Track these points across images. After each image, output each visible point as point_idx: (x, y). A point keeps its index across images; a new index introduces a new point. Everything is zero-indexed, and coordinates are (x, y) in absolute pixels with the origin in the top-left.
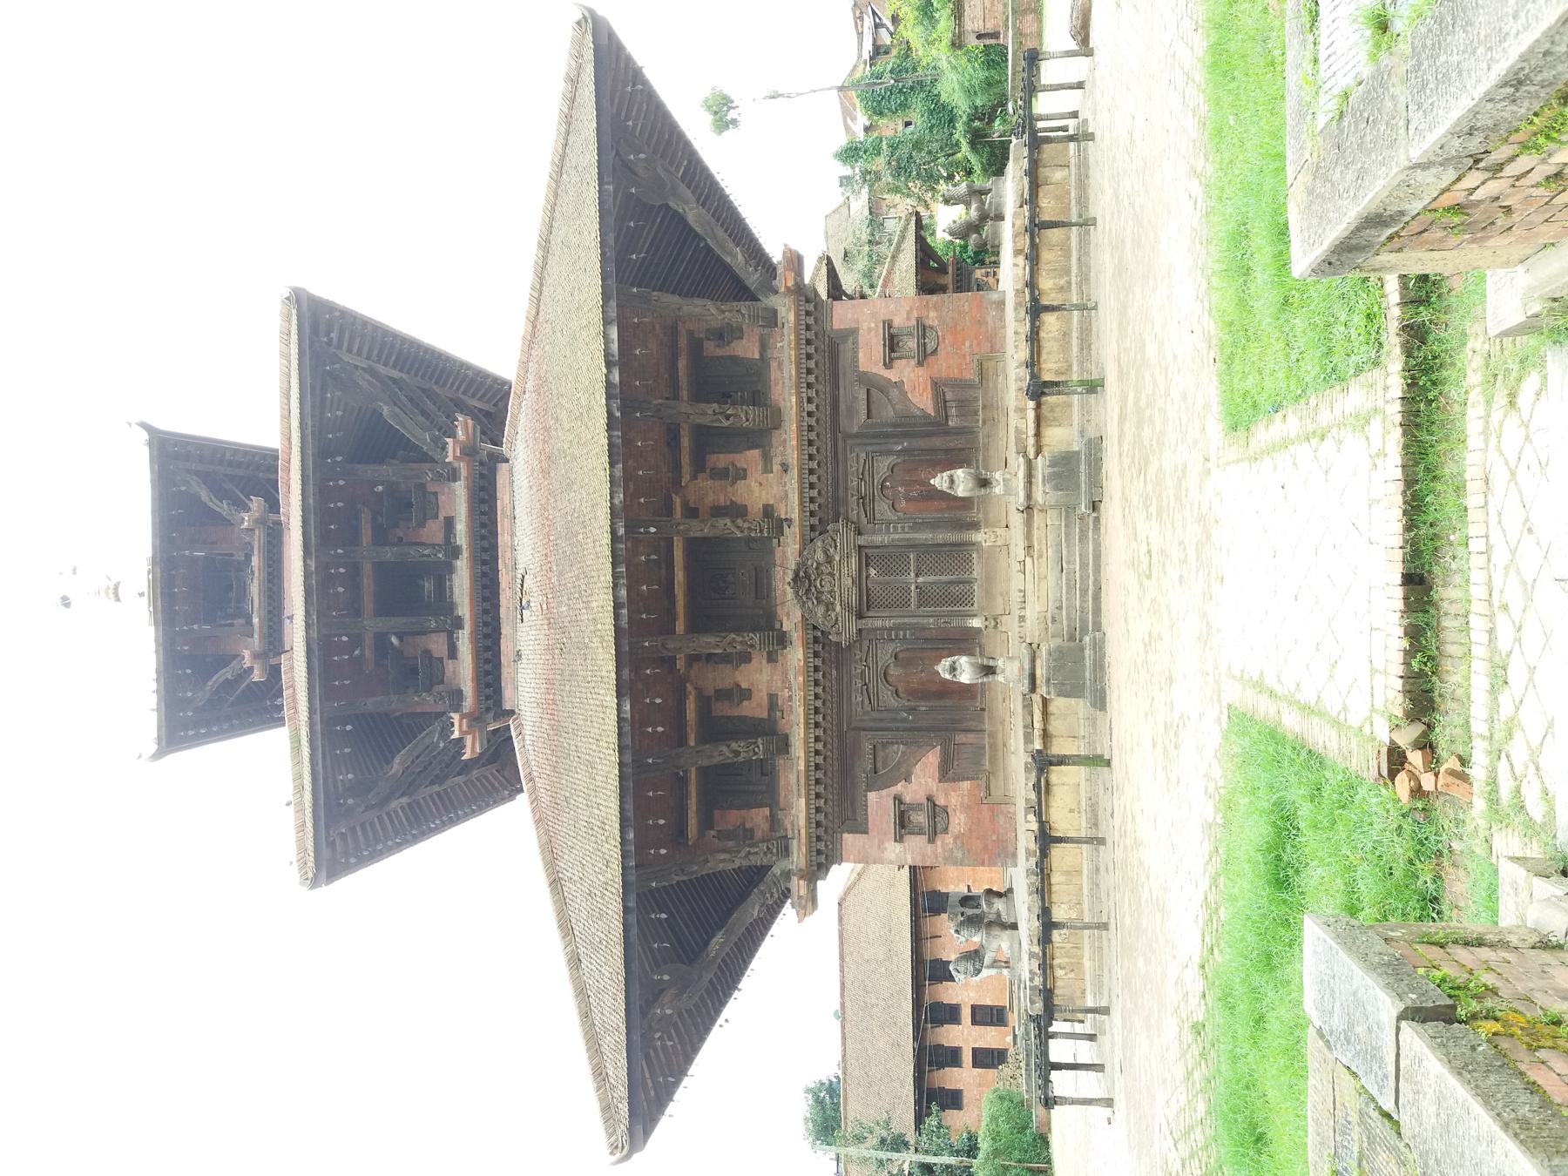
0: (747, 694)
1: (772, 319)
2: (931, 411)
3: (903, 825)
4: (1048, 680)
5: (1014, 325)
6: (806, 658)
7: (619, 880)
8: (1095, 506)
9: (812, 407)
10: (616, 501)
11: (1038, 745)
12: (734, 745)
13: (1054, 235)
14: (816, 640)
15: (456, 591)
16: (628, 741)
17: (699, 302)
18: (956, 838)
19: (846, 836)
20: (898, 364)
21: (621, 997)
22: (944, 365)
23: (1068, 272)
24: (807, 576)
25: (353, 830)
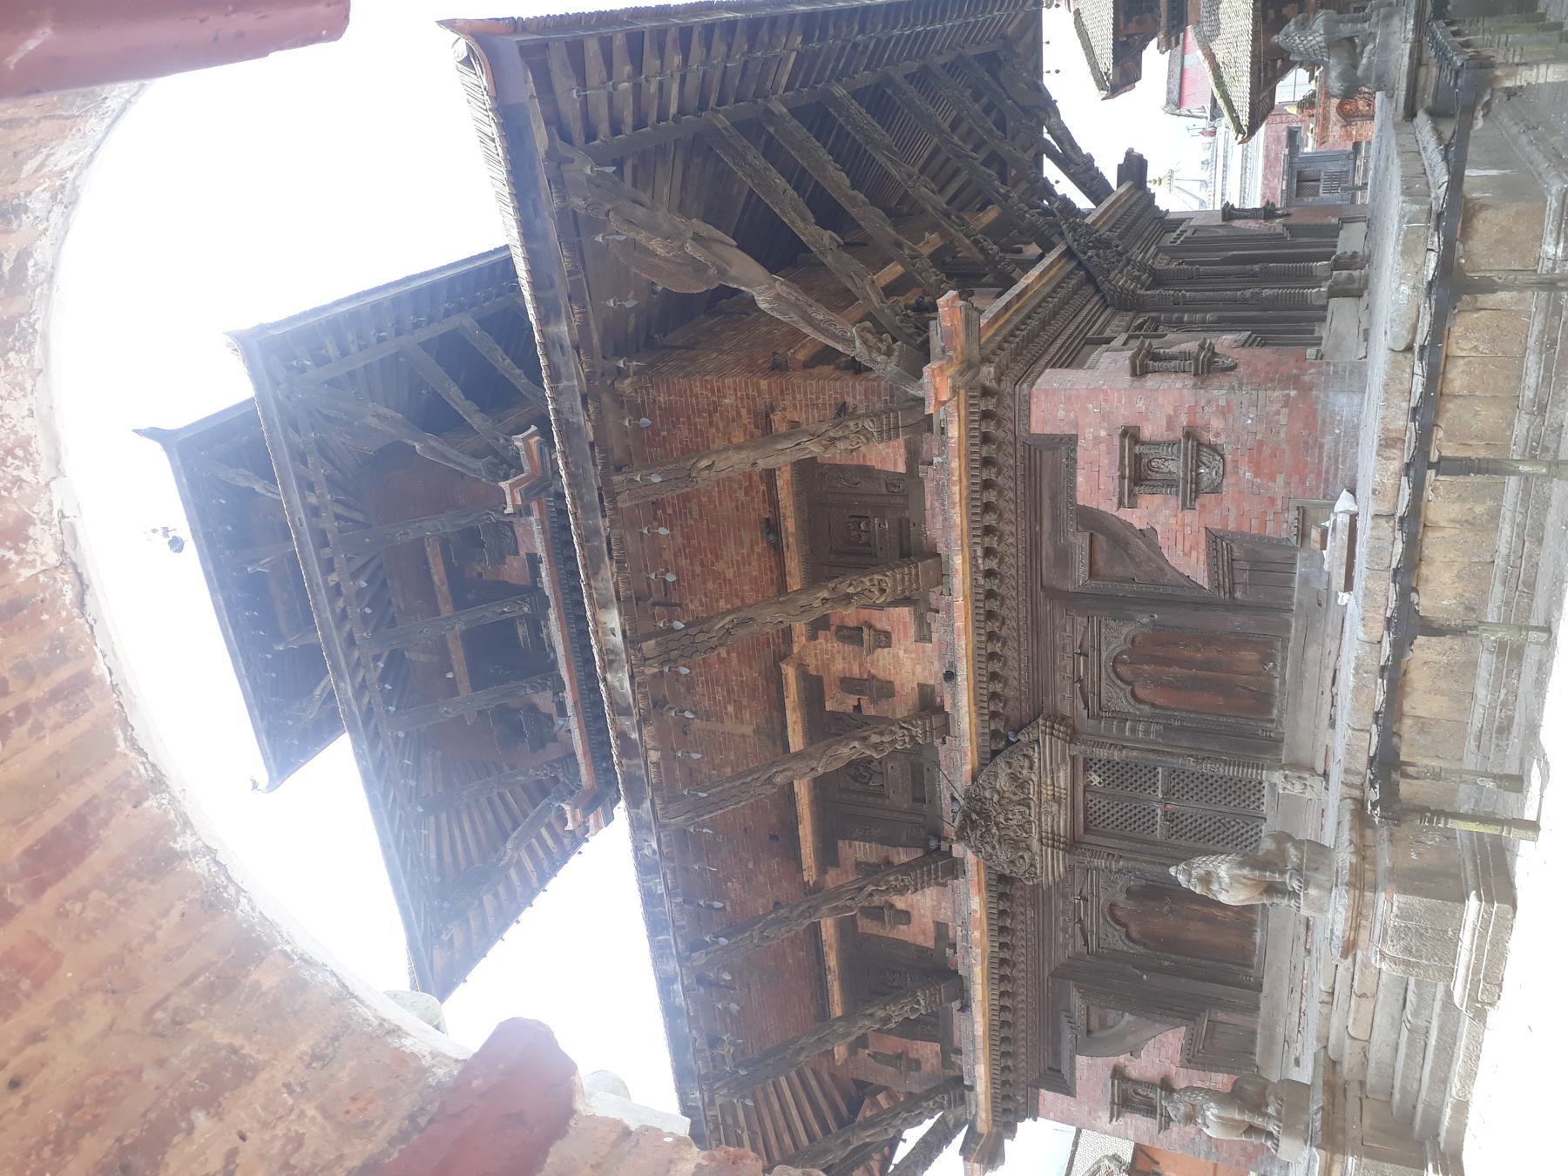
2: (1202, 579)
19: (1043, 1091)
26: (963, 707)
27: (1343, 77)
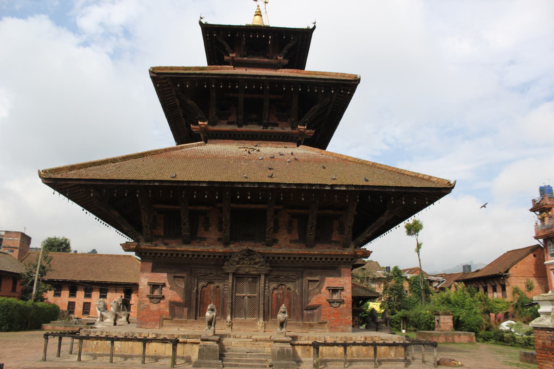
0: (207, 229)
1: (346, 246)
3: (154, 286)
4: (205, 346)
5: (339, 336)
6: (219, 252)
7: (141, 179)
8: (270, 366)
9: (313, 260)
10: (282, 185)
11: (181, 340)
12: (187, 224)
13: (372, 352)
14: (225, 257)
15: (252, 126)
16: (192, 185)
17: (353, 219)
18: (148, 306)
19: (151, 264)
20: (328, 291)
21: (98, 177)
22: (327, 309)
23: (358, 356)
24: (250, 255)
25: (169, 86)
26: (274, 250)
27: (381, 322)
